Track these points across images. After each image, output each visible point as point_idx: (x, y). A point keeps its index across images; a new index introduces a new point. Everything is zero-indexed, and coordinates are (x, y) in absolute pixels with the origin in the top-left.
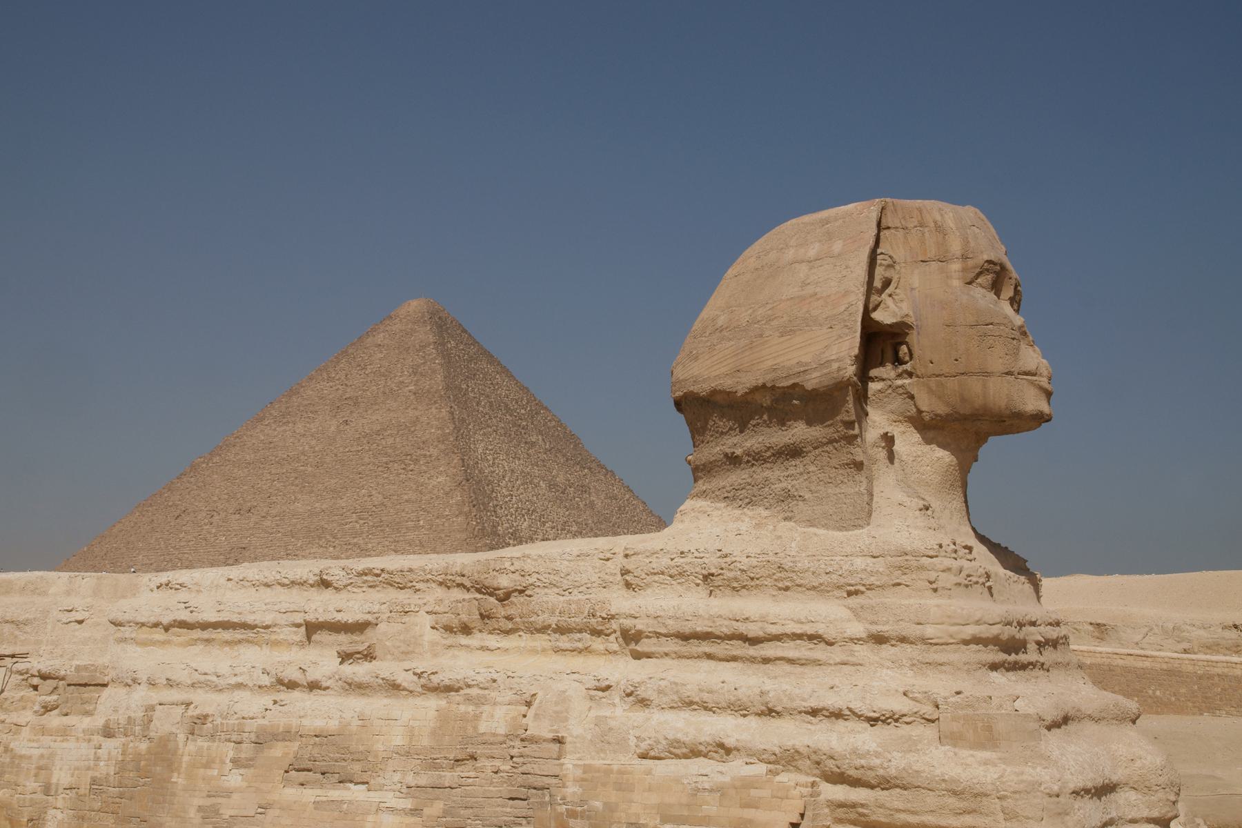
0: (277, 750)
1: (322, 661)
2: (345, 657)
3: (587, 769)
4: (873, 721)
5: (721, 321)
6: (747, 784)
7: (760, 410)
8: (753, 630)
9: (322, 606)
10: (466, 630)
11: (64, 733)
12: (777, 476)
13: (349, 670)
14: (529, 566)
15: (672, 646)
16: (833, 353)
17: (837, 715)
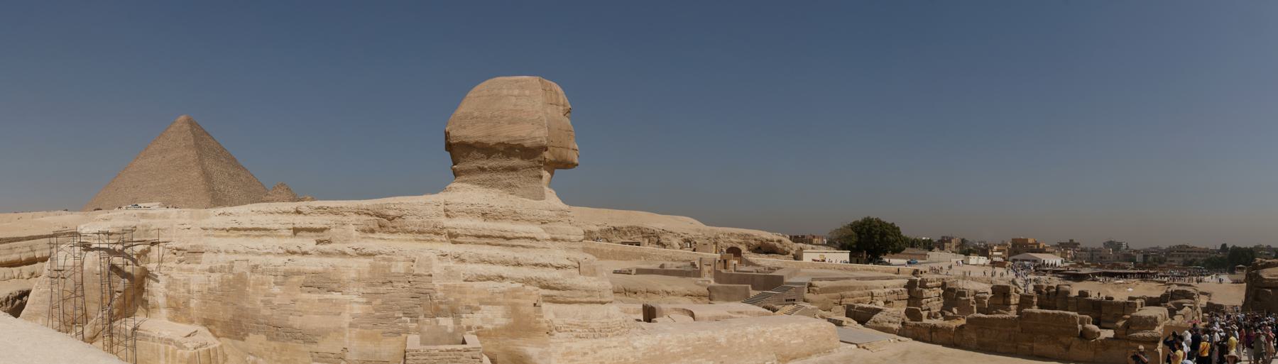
0: (296, 279)
1: (308, 243)
2: (318, 242)
3: (446, 286)
4: (557, 268)
5: (476, 114)
6: (514, 290)
7: (498, 152)
8: (509, 235)
9: (300, 221)
10: (372, 231)
11: (191, 270)
12: (505, 178)
13: (321, 247)
14: (403, 207)
15: (473, 240)
16: (537, 134)
17: (545, 266)
